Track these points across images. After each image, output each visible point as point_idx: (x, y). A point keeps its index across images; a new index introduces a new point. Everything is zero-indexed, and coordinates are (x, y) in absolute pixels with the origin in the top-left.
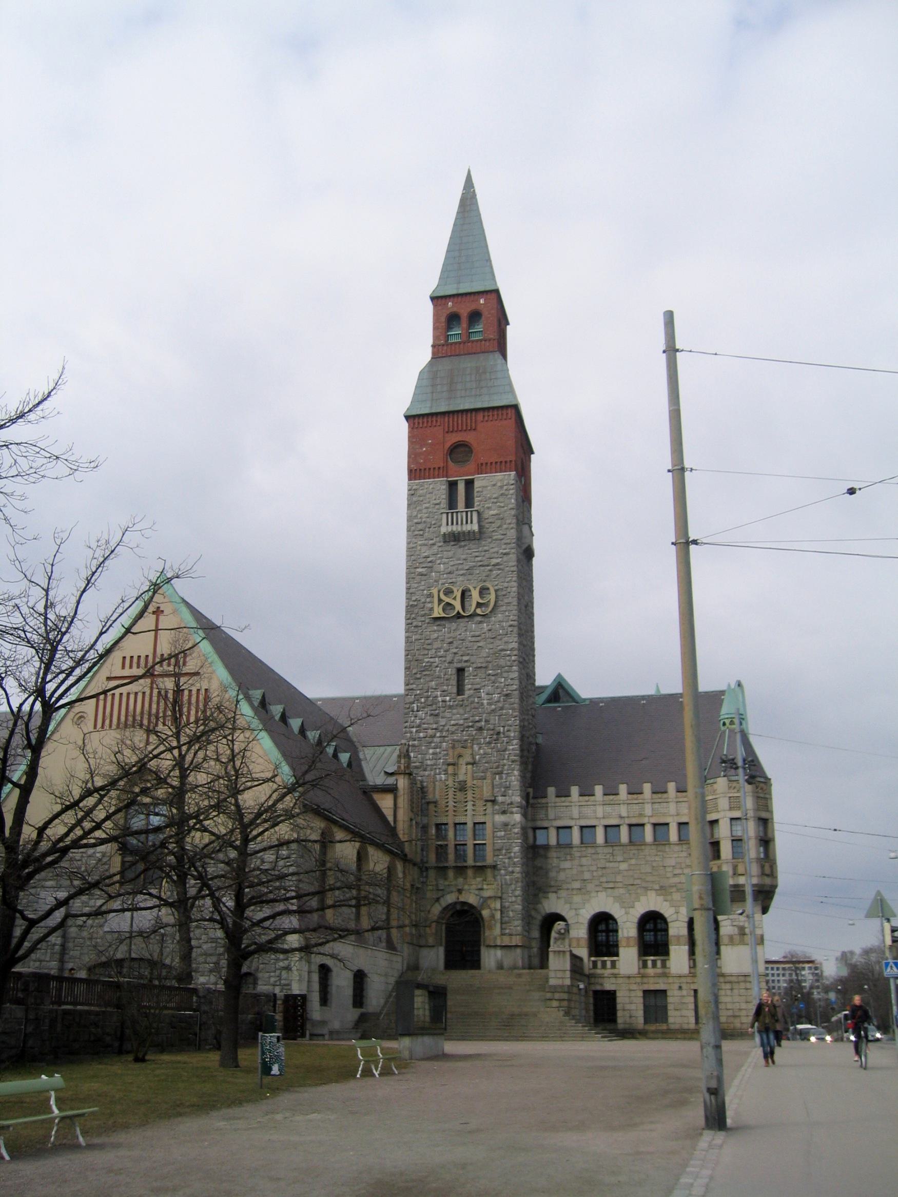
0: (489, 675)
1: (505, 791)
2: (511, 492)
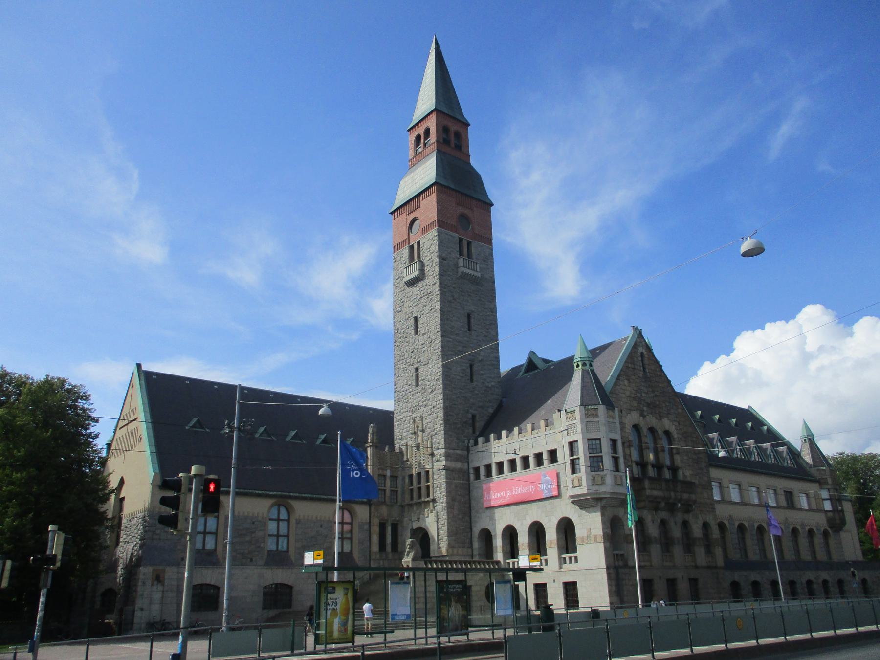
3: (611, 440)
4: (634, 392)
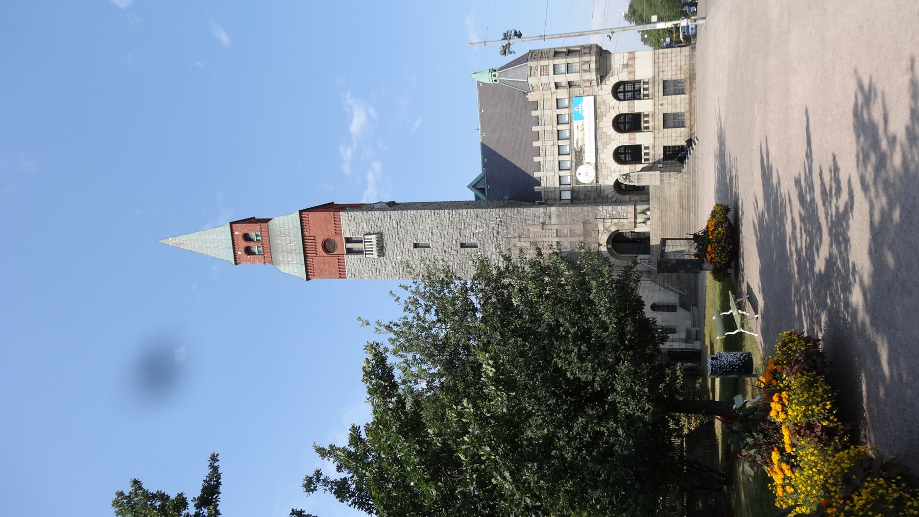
0: (464, 227)
1: (537, 217)
2: (352, 214)
3: (554, 56)
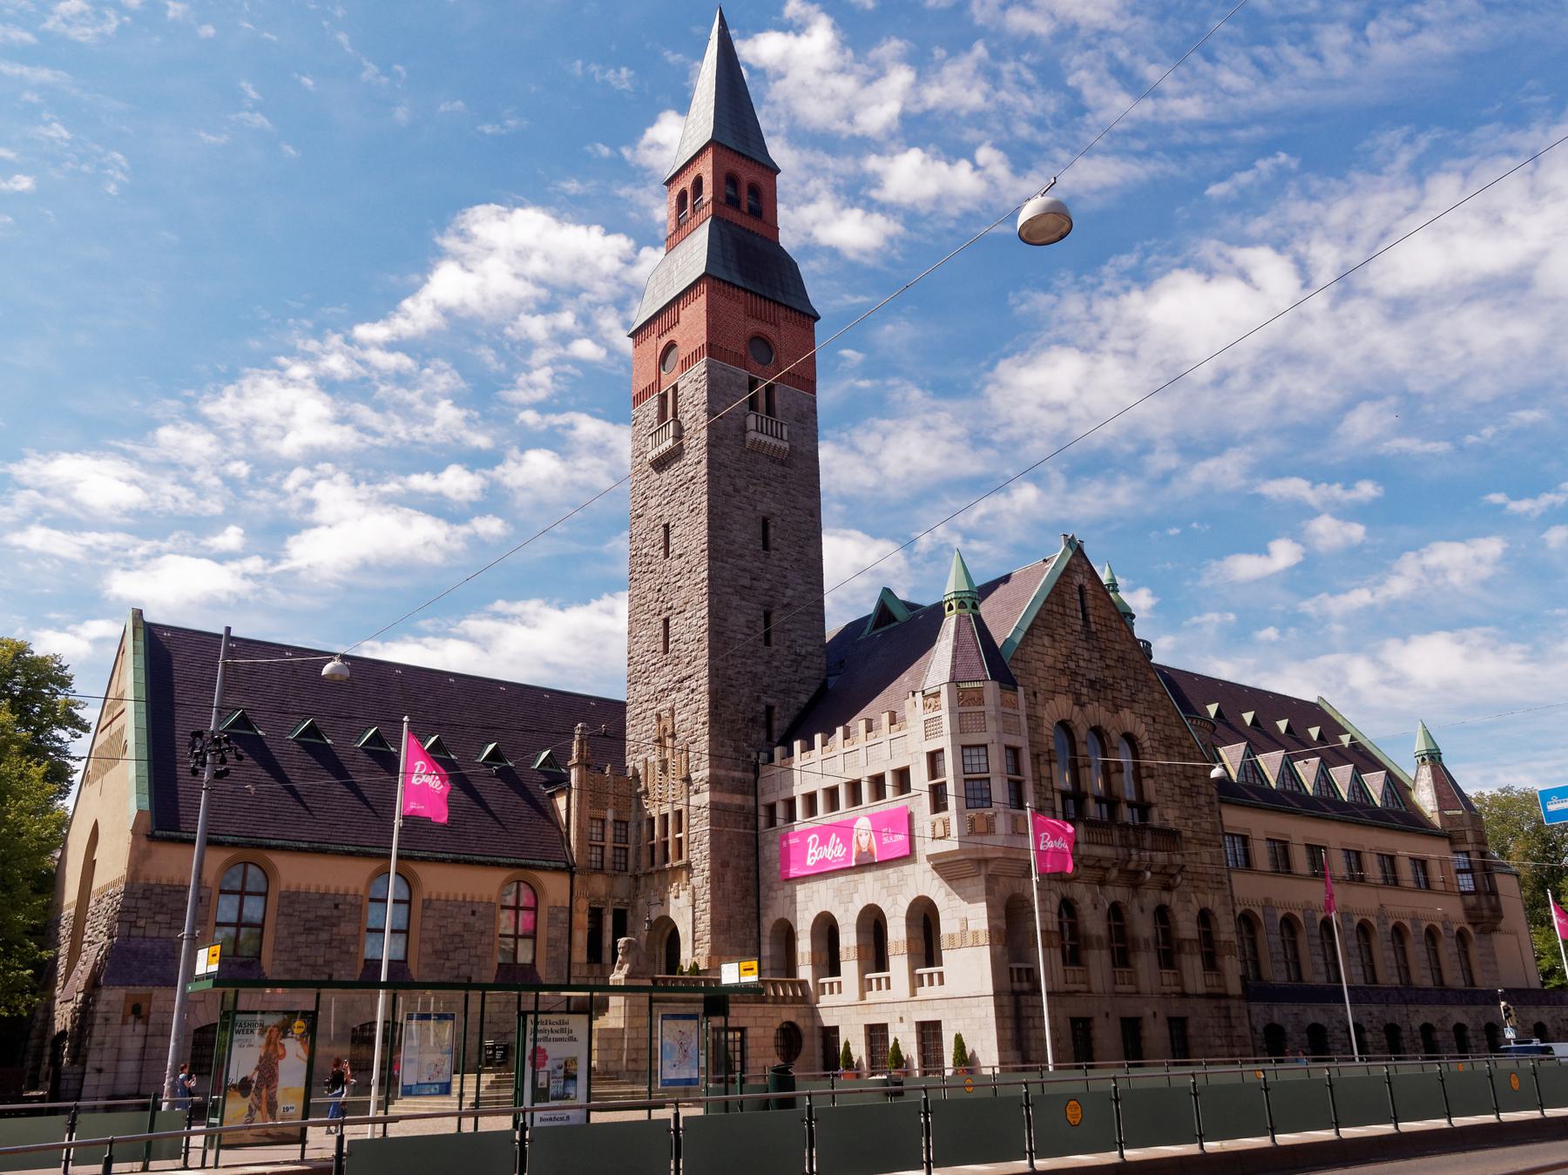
4: (1061, 659)
